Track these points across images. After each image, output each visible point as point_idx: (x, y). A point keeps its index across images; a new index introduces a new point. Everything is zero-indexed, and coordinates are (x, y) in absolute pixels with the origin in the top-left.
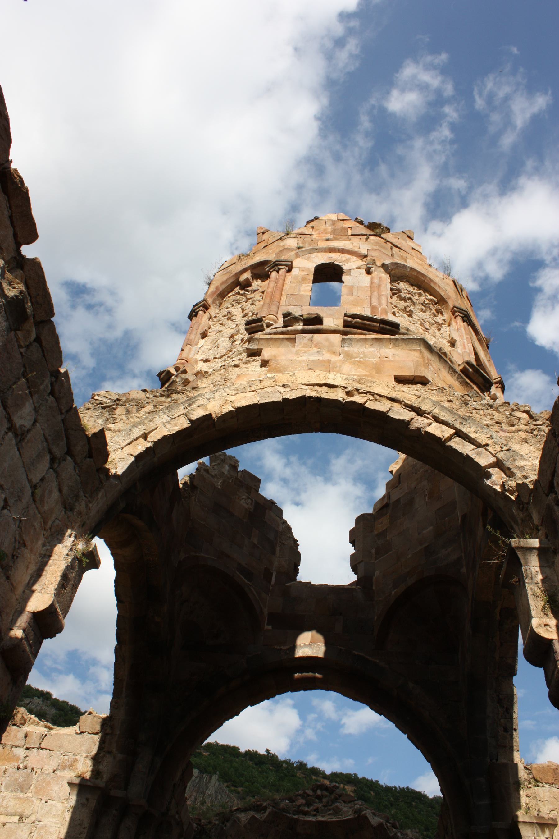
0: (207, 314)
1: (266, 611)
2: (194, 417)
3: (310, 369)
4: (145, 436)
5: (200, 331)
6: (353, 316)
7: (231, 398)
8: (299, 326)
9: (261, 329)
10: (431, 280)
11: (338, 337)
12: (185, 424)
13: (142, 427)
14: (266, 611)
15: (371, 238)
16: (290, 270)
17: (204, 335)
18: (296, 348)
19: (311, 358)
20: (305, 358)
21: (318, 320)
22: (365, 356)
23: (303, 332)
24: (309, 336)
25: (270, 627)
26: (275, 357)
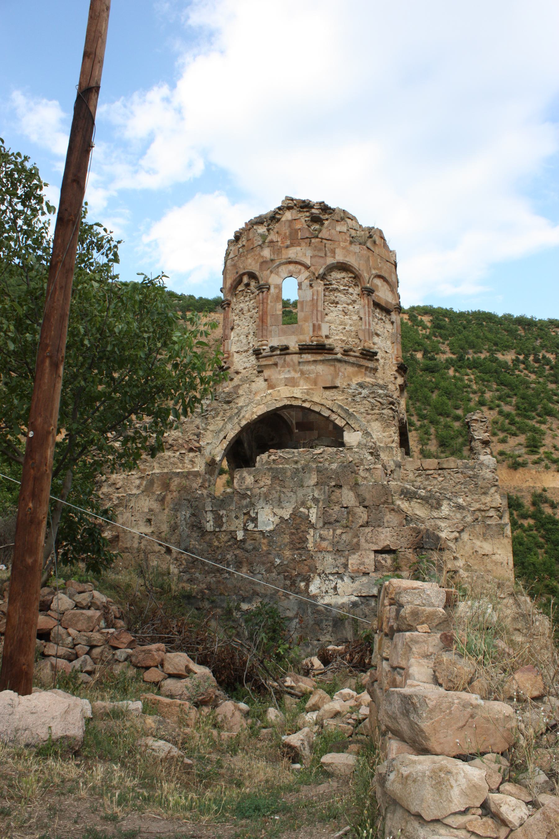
0: (231, 309)
1: (294, 422)
2: (242, 426)
3: (286, 385)
4: (225, 438)
5: (230, 328)
6: (302, 345)
7: (255, 410)
8: (278, 352)
9: (261, 354)
10: (350, 265)
11: (297, 355)
12: (240, 429)
13: (222, 433)
14: (294, 422)
15: (313, 240)
16: (269, 289)
17: (232, 329)
18: (279, 368)
19: (286, 376)
20: (283, 377)
21: (287, 348)
22: (310, 373)
23: (280, 355)
24: (283, 357)
25: (297, 431)
26: (269, 376)
